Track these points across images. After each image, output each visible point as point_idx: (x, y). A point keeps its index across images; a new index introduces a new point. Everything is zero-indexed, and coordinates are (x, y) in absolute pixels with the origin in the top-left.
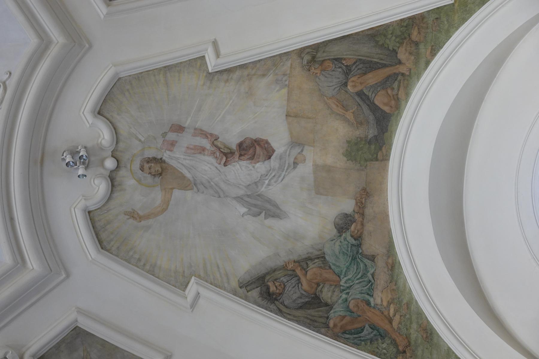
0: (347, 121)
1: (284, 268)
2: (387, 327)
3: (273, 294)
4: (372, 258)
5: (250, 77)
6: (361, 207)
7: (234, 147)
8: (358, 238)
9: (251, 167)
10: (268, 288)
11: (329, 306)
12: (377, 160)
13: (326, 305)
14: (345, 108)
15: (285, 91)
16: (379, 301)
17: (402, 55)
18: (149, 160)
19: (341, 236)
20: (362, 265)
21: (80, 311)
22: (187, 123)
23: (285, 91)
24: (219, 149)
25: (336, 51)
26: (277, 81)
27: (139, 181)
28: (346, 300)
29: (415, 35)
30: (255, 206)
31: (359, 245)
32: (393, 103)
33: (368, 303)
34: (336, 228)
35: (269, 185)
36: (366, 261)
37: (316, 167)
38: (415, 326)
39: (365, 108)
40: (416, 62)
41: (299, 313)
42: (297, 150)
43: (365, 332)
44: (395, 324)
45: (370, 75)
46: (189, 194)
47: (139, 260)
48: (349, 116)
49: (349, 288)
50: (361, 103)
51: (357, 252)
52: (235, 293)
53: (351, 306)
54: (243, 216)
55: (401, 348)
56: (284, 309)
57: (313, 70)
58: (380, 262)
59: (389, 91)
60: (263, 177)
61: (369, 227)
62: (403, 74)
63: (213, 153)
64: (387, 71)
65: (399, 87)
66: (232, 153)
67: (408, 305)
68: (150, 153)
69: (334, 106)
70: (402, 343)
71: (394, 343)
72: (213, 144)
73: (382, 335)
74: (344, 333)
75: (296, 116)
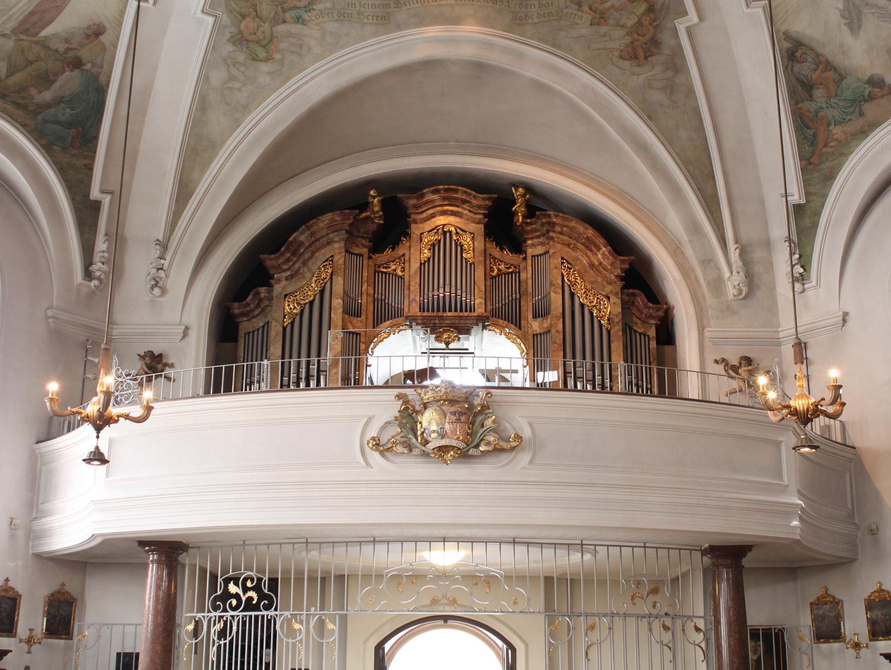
3: (795, 56)
13: (811, 96)
16: (834, 131)
19: (865, 84)
28: (823, 108)
31: (866, 101)
34: (869, 78)
36: (857, 110)
51: (860, 102)
54: (836, 8)
55: (811, 161)
71: (813, 153)
74: (800, 117)
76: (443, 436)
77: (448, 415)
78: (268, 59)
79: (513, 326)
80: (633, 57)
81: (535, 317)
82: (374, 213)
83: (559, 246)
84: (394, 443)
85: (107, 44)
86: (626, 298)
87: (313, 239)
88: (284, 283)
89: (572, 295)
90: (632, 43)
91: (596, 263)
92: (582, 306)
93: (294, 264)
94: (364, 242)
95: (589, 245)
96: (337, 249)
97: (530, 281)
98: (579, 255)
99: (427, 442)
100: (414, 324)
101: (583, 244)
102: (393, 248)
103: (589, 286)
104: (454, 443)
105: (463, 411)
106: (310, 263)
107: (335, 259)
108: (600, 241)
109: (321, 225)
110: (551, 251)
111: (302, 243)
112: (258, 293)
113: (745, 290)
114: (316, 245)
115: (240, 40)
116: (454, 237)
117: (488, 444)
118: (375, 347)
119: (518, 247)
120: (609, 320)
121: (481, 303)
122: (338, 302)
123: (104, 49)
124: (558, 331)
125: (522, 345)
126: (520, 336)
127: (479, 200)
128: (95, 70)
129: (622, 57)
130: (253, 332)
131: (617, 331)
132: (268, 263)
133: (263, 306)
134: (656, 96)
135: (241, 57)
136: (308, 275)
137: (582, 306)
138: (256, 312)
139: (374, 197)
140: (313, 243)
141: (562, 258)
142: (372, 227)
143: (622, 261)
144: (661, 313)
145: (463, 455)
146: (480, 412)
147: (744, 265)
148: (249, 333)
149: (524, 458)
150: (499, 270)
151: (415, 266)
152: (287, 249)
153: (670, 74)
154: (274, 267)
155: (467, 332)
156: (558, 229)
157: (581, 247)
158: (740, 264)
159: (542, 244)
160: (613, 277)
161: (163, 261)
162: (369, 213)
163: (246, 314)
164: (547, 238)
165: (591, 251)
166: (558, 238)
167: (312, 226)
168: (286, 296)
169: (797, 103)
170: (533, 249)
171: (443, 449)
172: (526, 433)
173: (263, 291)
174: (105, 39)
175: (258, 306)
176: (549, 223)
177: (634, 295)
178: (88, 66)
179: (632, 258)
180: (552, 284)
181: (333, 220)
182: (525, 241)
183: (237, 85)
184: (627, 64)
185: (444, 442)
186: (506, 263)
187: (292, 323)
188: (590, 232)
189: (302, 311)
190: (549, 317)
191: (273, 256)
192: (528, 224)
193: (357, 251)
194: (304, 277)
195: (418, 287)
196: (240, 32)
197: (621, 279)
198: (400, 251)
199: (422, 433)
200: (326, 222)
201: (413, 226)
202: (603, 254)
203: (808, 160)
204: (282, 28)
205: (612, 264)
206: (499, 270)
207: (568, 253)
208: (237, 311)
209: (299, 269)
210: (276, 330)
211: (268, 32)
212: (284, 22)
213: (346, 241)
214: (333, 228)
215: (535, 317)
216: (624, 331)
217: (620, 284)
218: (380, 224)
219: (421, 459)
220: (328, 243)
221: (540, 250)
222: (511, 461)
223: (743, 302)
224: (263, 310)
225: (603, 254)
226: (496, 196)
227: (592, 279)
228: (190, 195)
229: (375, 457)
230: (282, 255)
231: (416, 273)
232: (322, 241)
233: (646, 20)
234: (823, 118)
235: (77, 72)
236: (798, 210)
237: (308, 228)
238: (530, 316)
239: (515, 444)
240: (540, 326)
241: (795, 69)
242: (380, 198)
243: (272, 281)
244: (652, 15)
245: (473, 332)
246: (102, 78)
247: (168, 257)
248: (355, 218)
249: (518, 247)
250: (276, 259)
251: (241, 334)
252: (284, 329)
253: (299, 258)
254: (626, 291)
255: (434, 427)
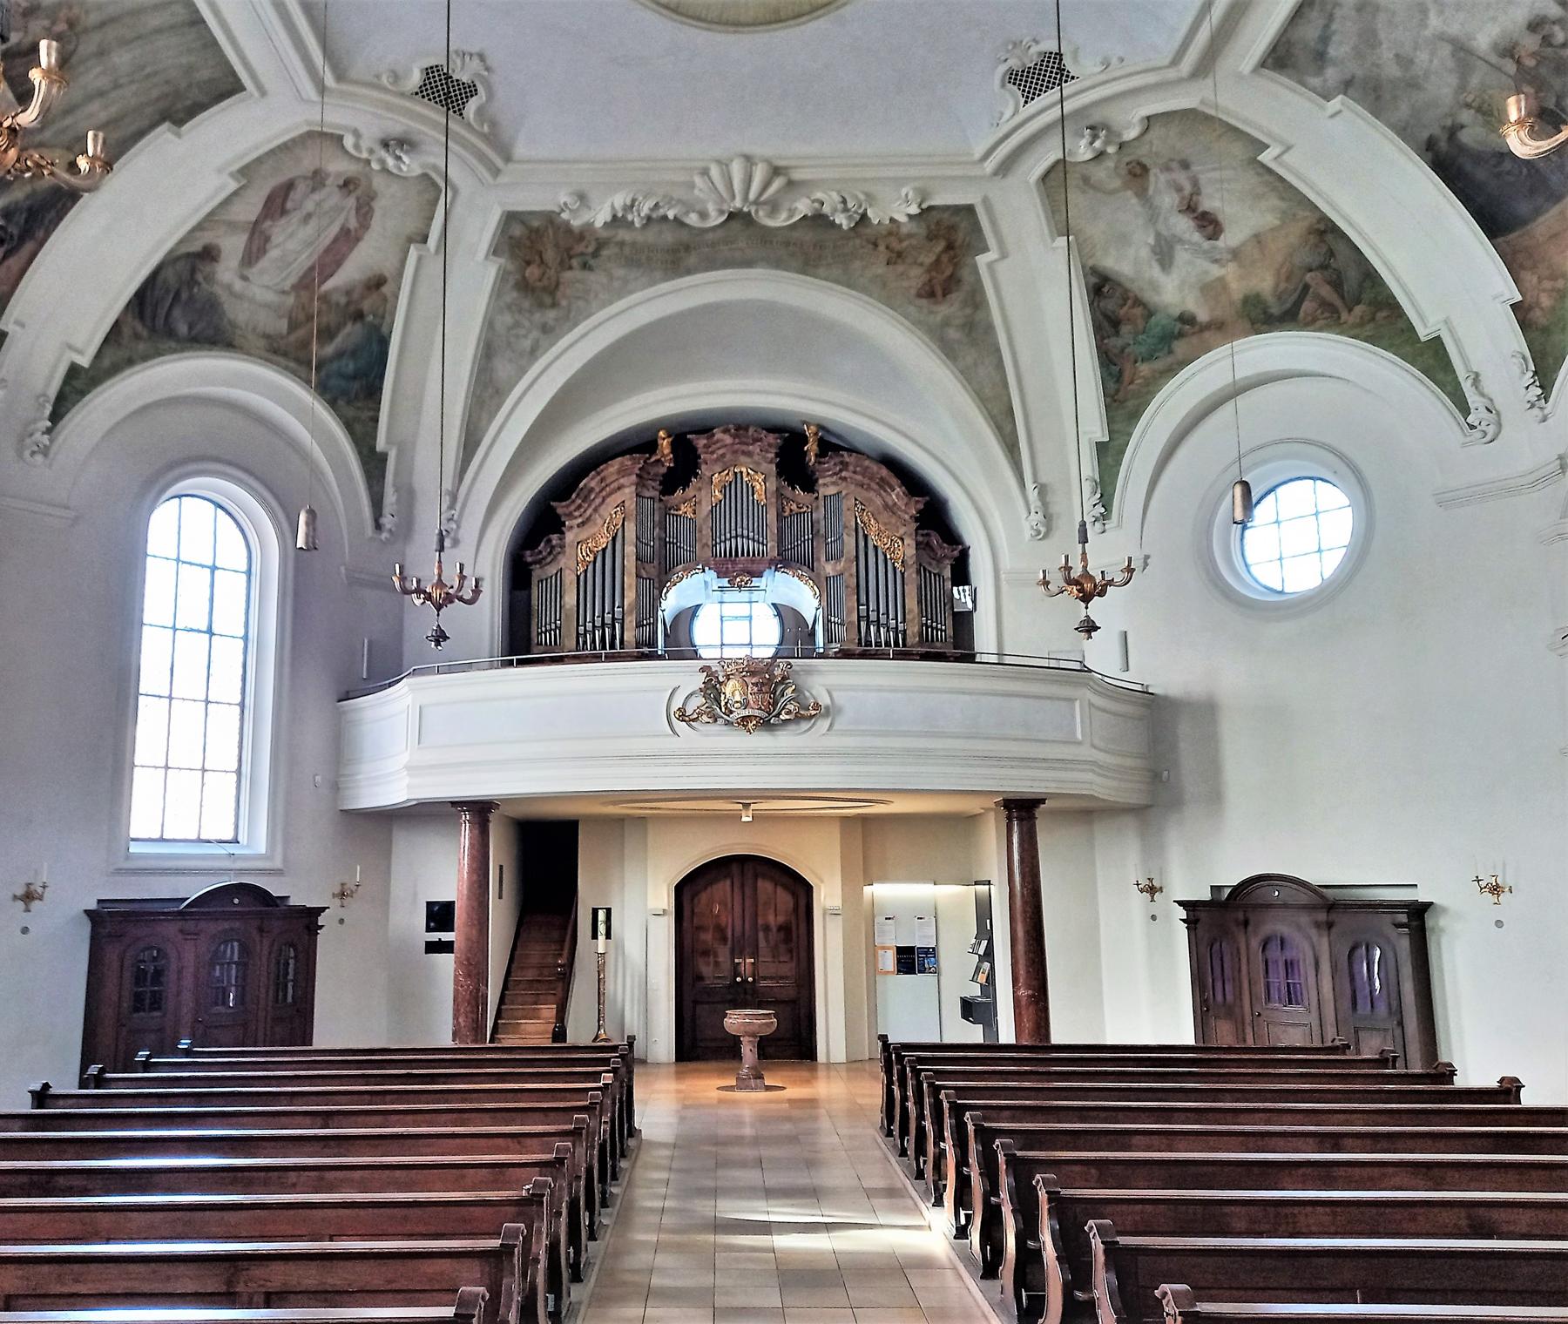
0: (1277, 285)
1: (1126, 291)
2: (1125, 383)
4: (1170, 352)
5: (1274, 189)
6: (1207, 327)
7: (1201, 209)
8: (1181, 335)
9: (1192, 229)
10: (1104, 286)
11: (1117, 333)
12: (1253, 324)
14: (1288, 279)
15: (1277, 222)
17: (1358, 310)
18: (1139, 163)
20: (1160, 346)
21: (986, 201)
22: (1195, 168)
23: (1277, 222)
24: (1191, 200)
25: (1340, 247)
26: (1284, 212)
27: (1116, 167)
29: (1381, 315)
30: (1161, 247)
32: (1310, 318)
33: (1136, 362)
35: (1186, 249)
37: (1221, 280)
38: (1136, 402)
39: (1296, 295)
40: (1355, 326)
41: (1098, 314)
42: (1229, 257)
43: (1114, 367)
44: (1131, 387)
45: (1328, 288)
46: (1134, 201)
47: (1055, 201)
48: (1283, 286)
49: (1140, 343)
50: (1298, 292)
52: (1083, 267)
53: (1127, 350)
56: (1095, 304)
57: (1312, 236)
58: (1170, 360)
59: (1319, 311)
60: (1190, 243)
61: (1194, 340)
62: (1339, 318)
63: (1183, 198)
64: (1338, 303)
65: (1326, 318)
66: (1194, 211)
67: (1147, 393)
68: (1145, 161)
69: (1284, 270)
70: (1120, 396)
72: (1192, 195)
73: (1119, 378)
75: (1259, 242)
76: (746, 705)
77: (750, 686)
78: (554, 305)
79: (805, 568)
80: (931, 295)
81: (827, 560)
82: (663, 456)
83: (853, 487)
84: (699, 714)
85: (389, 295)
86: (920, 539)
87: (603, 484)
88: (576, 530)
89: (866, 537)
90: (930, 281)
91: (890, 503)
92: (876, 548)
93: (585, 511)
94: (653, 484)
95: (883, 483)
96: (628, 493)
97: (822, 523)
98: (872, 494)
99: (731, 712)
100: (707, 569)
101: (878, 483)
102: (684, 490)
103: (883, 528)
104: (757, 713)
105: (765, 681)
106: (601, 510)
107: (626, 504)
108: (894, 481)
109: (611, 470)
110: (844, 493)
111: (592, 490)
112: (549, 541)
113: (1043, 530)
114: (607, 491)
115: (524, 286)
116: (745, 479)
117: (789, 713)
118: (668, 591)
119: (809, 485)
120: (902, 562)
121: (773, 546)
122: (630, 549)
123: (385, 299)
124: (851, 575)
125: (815, 588)
126: (813, 578)
127: (771, 438)
128: (377, 322)
129: (919, 295)
130: (546, 580)
131: (911, 574)
132: (559, 511)
133: (554, 552)
134: (953, 334)
135: (526, 304)
136: (600, 521)
137: (876, 548)
138: (549, 559)
139: (664, 439)
140: (603, 489)
141: (856, 500)
142: (664, 470)
143: (917, 502)
144: (956, 553)
145: (766, 724)
146: (781, 682)
147: (1043, 505)
148: (542, 581)
149: (824, 724)
150: (791, 510)
151: (705, 508)
152: (578, 495)
153: (968, 311)
154: (566, 515)
155: (760, 575)
156: (851, 468)
157: (876, 487)
158: (1039, 504)
159: (834, 483)
160: (907, 517)
161: (453, 512)
162: (659, 457)
163: (539, 562)
164: (840, 478)
165: (885, 491)
166: (851, 478)
167: (602, 471)
168: (578, 543)
169: (1103, 338)
170: (827, 487)
171: (745, 720)
172: (824, 700)
173: (555, 538)
174: (385, 289)
175: (550, 553)
176: (842, 463)
177: (928, 535)
178: (370, 318)
179: (927, 498)
180: (846, 527)
181: (622, 464)
182: (817, 480)
183: (522, 332)
184: (924, 302)
185: (746, 713)
186: (798, 504)
187: (586, 571)
188: (884, 472)
189: (595, 558)
190: (843, 559)
191: (564, 503)
192: (820, 463)
193: (647, 494)
194: (595, 524)
195: (709, 530)
196: (524, 278)
197: (916, 520)
198: (690, 492)
199: (726, 703)
200: (616, 467)
201: (704, 467)
202: (897, 495)
203: (1112, 397)
204: (568, 275)
205: (906, 504)
206: (791, 510)
207: (863, 494)
208: (529, 559)
209: (590, 516)
210: (569, 579)
211: (554, 279)
212: (570, 268)
213: (637, 485)
214: (623, 472)
215: (827, 560)
216: (918, 572)
217: (915, 525)
218: (669, 467)
219: (725, 728)
220: (619, 488)
221: (832, 490)
222: (811, 728)
223: (1041, 542)
224: (555, 557)
225: (897, 495)
226: (787, 435)
227: (886, 521)
228: (477, 444)
229: (681, 726)
230: (573, 501)
231: (708, 515)
232: (612, 486)
233: (945, 258)
234: (1129, 355)
235: (358, 326)
236: (1101, 448)
237: (598, 474)
238: (823, 559)
239: (813, 712)
240: (834, 569)
241: (1101, 304)
242: (670, 440)
243: (563, 529)
244: (952, 253)
245: (765, 574)
246: (384, 330)
247: (458, 506)
248: (645, 462)
249: (809, 485)
250: (568, 506)
251: (534, 581)
252: (578, 577)
253: (589, 506)
254: (920, 532)
255: (738, 698)
